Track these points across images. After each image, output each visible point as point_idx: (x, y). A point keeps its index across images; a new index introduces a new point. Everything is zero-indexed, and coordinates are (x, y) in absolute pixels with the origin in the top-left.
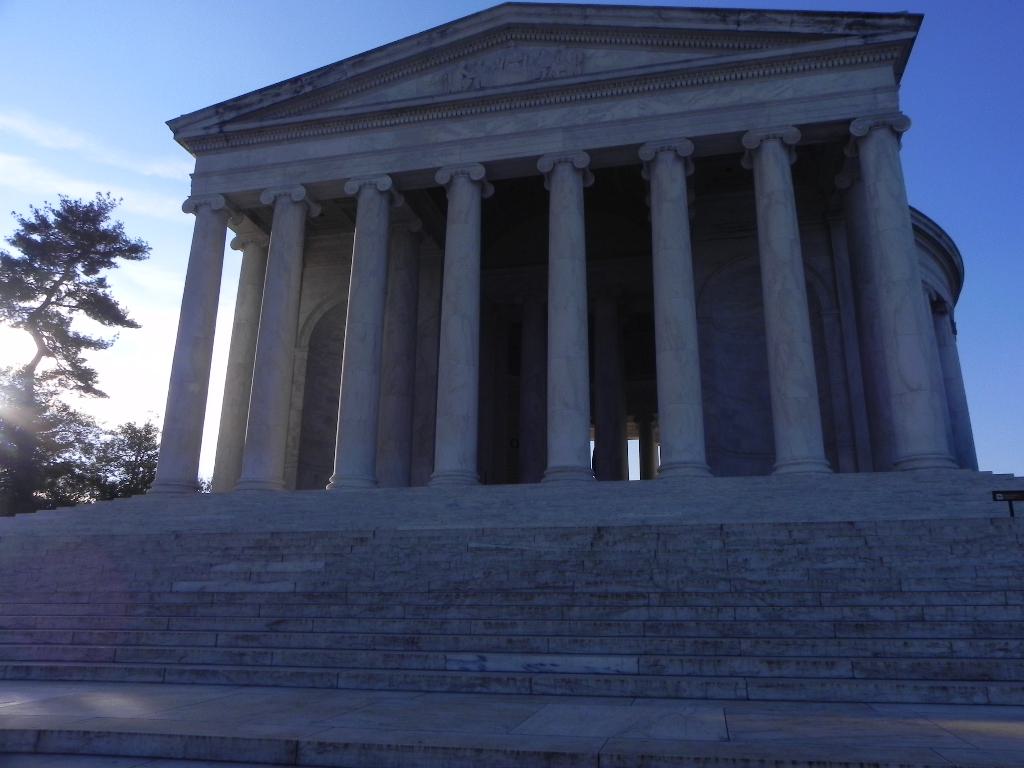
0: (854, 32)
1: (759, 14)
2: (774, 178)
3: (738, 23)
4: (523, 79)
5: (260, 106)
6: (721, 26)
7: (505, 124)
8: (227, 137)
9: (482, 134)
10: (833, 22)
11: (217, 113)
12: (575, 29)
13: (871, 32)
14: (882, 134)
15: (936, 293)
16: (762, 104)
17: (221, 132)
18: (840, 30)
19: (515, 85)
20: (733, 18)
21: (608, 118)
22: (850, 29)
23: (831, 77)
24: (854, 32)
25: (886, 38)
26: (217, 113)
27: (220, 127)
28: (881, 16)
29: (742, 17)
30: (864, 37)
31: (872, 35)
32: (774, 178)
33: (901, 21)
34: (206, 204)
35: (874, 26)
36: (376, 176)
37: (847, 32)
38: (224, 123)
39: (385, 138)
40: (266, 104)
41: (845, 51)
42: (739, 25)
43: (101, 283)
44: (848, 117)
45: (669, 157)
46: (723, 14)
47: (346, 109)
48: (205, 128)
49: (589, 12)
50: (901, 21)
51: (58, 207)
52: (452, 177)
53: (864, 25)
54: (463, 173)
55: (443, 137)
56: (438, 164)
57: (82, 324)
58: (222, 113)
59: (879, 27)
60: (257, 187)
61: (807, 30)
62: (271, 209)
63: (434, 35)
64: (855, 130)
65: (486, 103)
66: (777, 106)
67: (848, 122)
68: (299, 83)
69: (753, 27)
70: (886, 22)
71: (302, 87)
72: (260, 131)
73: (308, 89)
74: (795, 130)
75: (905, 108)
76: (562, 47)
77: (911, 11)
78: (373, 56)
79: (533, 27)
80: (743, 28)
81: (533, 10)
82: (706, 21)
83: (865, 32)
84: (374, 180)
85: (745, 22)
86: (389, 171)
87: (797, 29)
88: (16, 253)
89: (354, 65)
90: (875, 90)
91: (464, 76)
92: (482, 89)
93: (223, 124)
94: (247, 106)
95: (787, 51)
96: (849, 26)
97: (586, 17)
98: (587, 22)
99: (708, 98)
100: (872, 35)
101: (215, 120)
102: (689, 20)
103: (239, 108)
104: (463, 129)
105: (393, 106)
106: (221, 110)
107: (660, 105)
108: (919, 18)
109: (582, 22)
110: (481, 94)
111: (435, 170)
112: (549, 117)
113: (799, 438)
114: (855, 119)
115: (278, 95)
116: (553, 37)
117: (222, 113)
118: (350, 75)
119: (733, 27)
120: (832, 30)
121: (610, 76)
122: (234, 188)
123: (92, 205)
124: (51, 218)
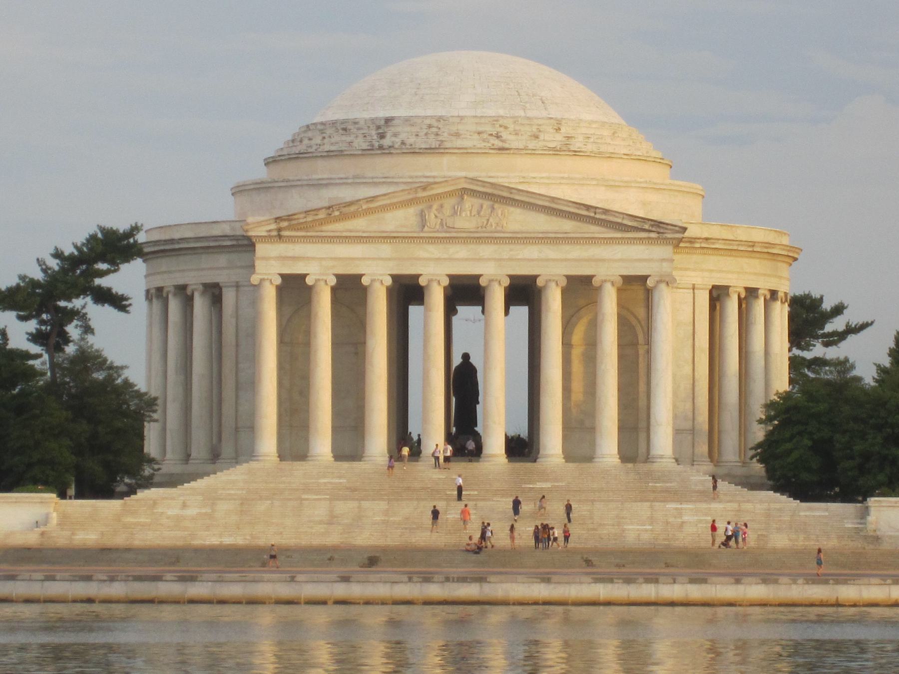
1: (606, 211)
2: (610, 304)
7: (460, 251)
8: (280, 237)
9: (446, 256)
14: (663, 286)
16: (603, 260)
18: (646, 227)
20: (593, 210)
24: (654, 229)
25: (669, 236)
28: (667, 224)
29: (598, 211)
30: (659, 233)
32: (610, 304)
33: (677, 228)
39: (386, 250)
41: (649, 238)
45: (553, 285)
46: (588, 207)
49: (513, 191)
50: (677, 228)
53: (659, 227)
55: (422, 254)
56: (420, 272)
61: (630, 224)
63: (419, 190)
65: (450, 237)
69: (603, 217)
70: (670, 227)
73: (337, 213)
76: (496, 206)
78: (379, 198)
80: (597, 216)
81: (480, 183)
83: (658, 230)
84: (381, 278)
85: (599, 213)
87: (626, 222)
89: (367, 202)
90: (663, 260)
91: (436, 217)
95: (619, 235)
98: (512, 196)
104: (434, 251)
107: (550, 252)
110: (448, 235)
112: (486, 250)
113: (608, 444)
118: (364, 207)
119: (592, 215)
122: (287, 271)
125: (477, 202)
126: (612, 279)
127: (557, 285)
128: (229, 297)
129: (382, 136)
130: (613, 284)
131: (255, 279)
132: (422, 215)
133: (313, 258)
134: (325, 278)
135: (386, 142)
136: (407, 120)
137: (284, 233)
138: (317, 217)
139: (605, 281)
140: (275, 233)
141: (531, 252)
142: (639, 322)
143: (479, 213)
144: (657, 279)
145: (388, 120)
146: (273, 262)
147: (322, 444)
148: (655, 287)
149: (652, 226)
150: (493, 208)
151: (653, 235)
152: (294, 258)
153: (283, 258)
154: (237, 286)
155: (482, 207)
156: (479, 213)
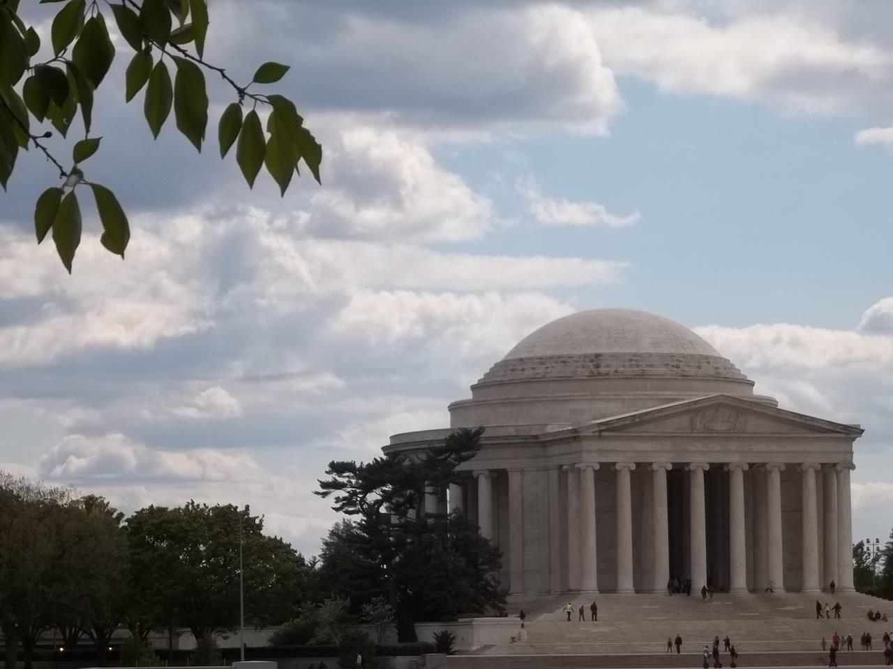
2: (811, 483)
3: (806, 420)
6: (799, 420)
13: (848, 432)
18: (838, 430)
21: (755, 449)
30: (846, 434)
32: (811, 483)
38: (601, 431)
39: (668, 445)
40: (619, 424)
41: (838, 438)
50: (859, 431)
55: (692, 448)
64: (838, 467)
66: (813, 453)
75: (855, 461)
77: (862, 428)
80: (807, 422)
91: (701, 422)
96: (842, 429)
99: (791, 447)
101: (596, 429)
104: (699, 446)
107: (774, 448)
108: (863, 431)
112: (733, 446)
119: (803, 421)
128: (514, 481)
129: (597, 366)
133: (620, 451)
134: (628, 465)
135: (603, 370)
136: (612, 356)
141: (761, 447)
145: (598, 356)
146: (594, 454)
147: (626, 582)
148: (841, 471)
149: (842, 429)
150: (737, 416)
151: (842, 435)
153: (600, 451)
154: (522, 471)
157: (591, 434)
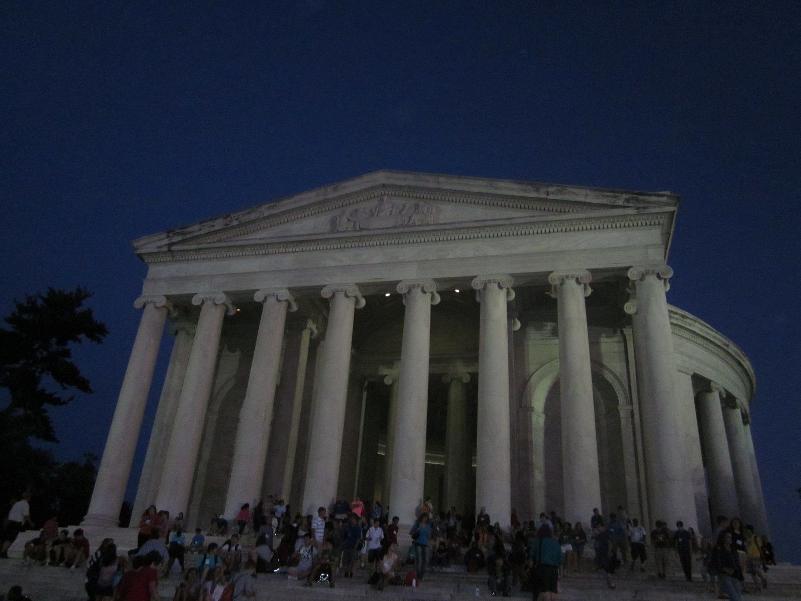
0: (630, 205)
4: (390, 226)
5: (199, 233)
10: (616, 197)
11: (168, 237)
12: (430, 190)
14: (652, 279)
15: (726, 390)
17: (169, 250)
18: (620, 203)
19: (383, 229)
21: (451, 256)
22: (628, 202)
23: (616, 234)
24: (630, 205)
26: (168, 237)
27: (169, 247)
30: (638, 208)
31: (644, 208)
34: (151, 302)
35: (644, 201)
36: (279, 289)
37: (626, 204)
39: (287, 260)
40: (203, 232)
42: (548, 195)
43: (67, 353)
44: (626, 265)
45: (495, 286)
47: (261, 239)
48: (158, 247)
51: (45, 295)
52: (334, 293)
54: (342, 291)
55: (330, 263)
56: (326, 283)
57: (48, 383)
58: (172, 237)
59: (649, 202)
60: (191, 292)
61: (596, 201)
62: (199, 308)
64: (631, 275)
67: (627, 268)
68: (229, 219)
69: (559, 197)
71: (231, 221)
72: (197, 250)
73: (235, 223)
74: (588, 272)
76: (421, 203)
79: (401, 187)
80: (551, 197)
82: (525, 191)
83: (639, 205)
84: (276, 292)
85: (553, 193)
86: (288, 286)
88: (9, 328)
90: (647, 247)
91: (349, 220)
92: (361, 229)
93: (171, 245)
94: (190, 232)
96: (627, 200)
97: (439, 183)
100: (644, 208)
101: (166, 242)
102: (513, 190)
103: (184, 234)
104: (345, 257)
105: (293, 239)
106: (171, 235)
107: (489, 248)
109: (436, 186)
111: (321, 287)
112: (408, 252)
114: (631, 267)
115: (213, 226)
116: (415, 195)
117: (172, 237)
119: (544, 196)
120: (615, 202)
121: (453, 226)
122: (174, 292)
123: (71, 294)
124: (40, 302)
125: (399, 202)
126: (577, 273)
127: (500, 287)
130: (578, 282)
131: (138, 303)
132: (333, 222)
137: (174, 248)
138: (212, 229)
139: (567, 277)
140: (166, 249)
142: (618, 379)
143: (400, 212)
144: (642, 270)
152: (187, 279)
155: (404, 206)
156: (400, 212)
157: (156, 250)
